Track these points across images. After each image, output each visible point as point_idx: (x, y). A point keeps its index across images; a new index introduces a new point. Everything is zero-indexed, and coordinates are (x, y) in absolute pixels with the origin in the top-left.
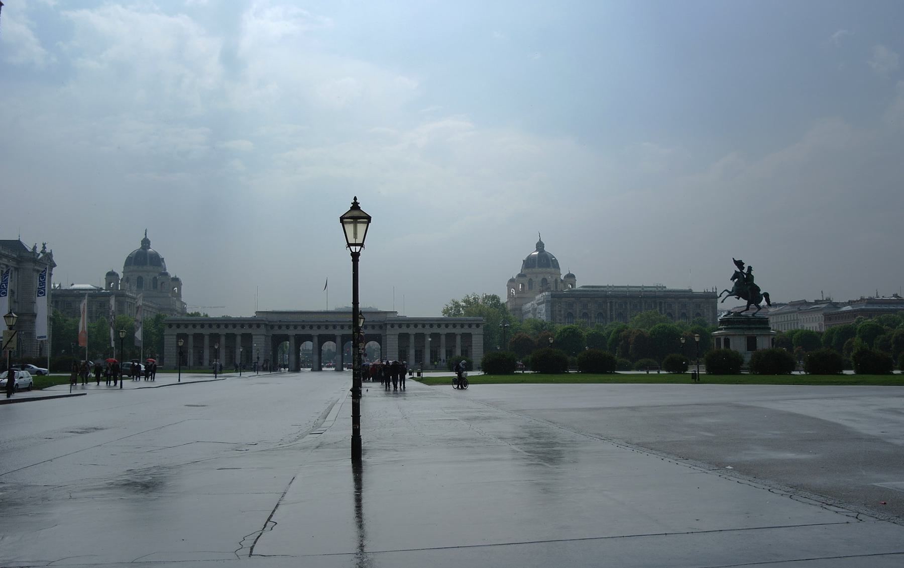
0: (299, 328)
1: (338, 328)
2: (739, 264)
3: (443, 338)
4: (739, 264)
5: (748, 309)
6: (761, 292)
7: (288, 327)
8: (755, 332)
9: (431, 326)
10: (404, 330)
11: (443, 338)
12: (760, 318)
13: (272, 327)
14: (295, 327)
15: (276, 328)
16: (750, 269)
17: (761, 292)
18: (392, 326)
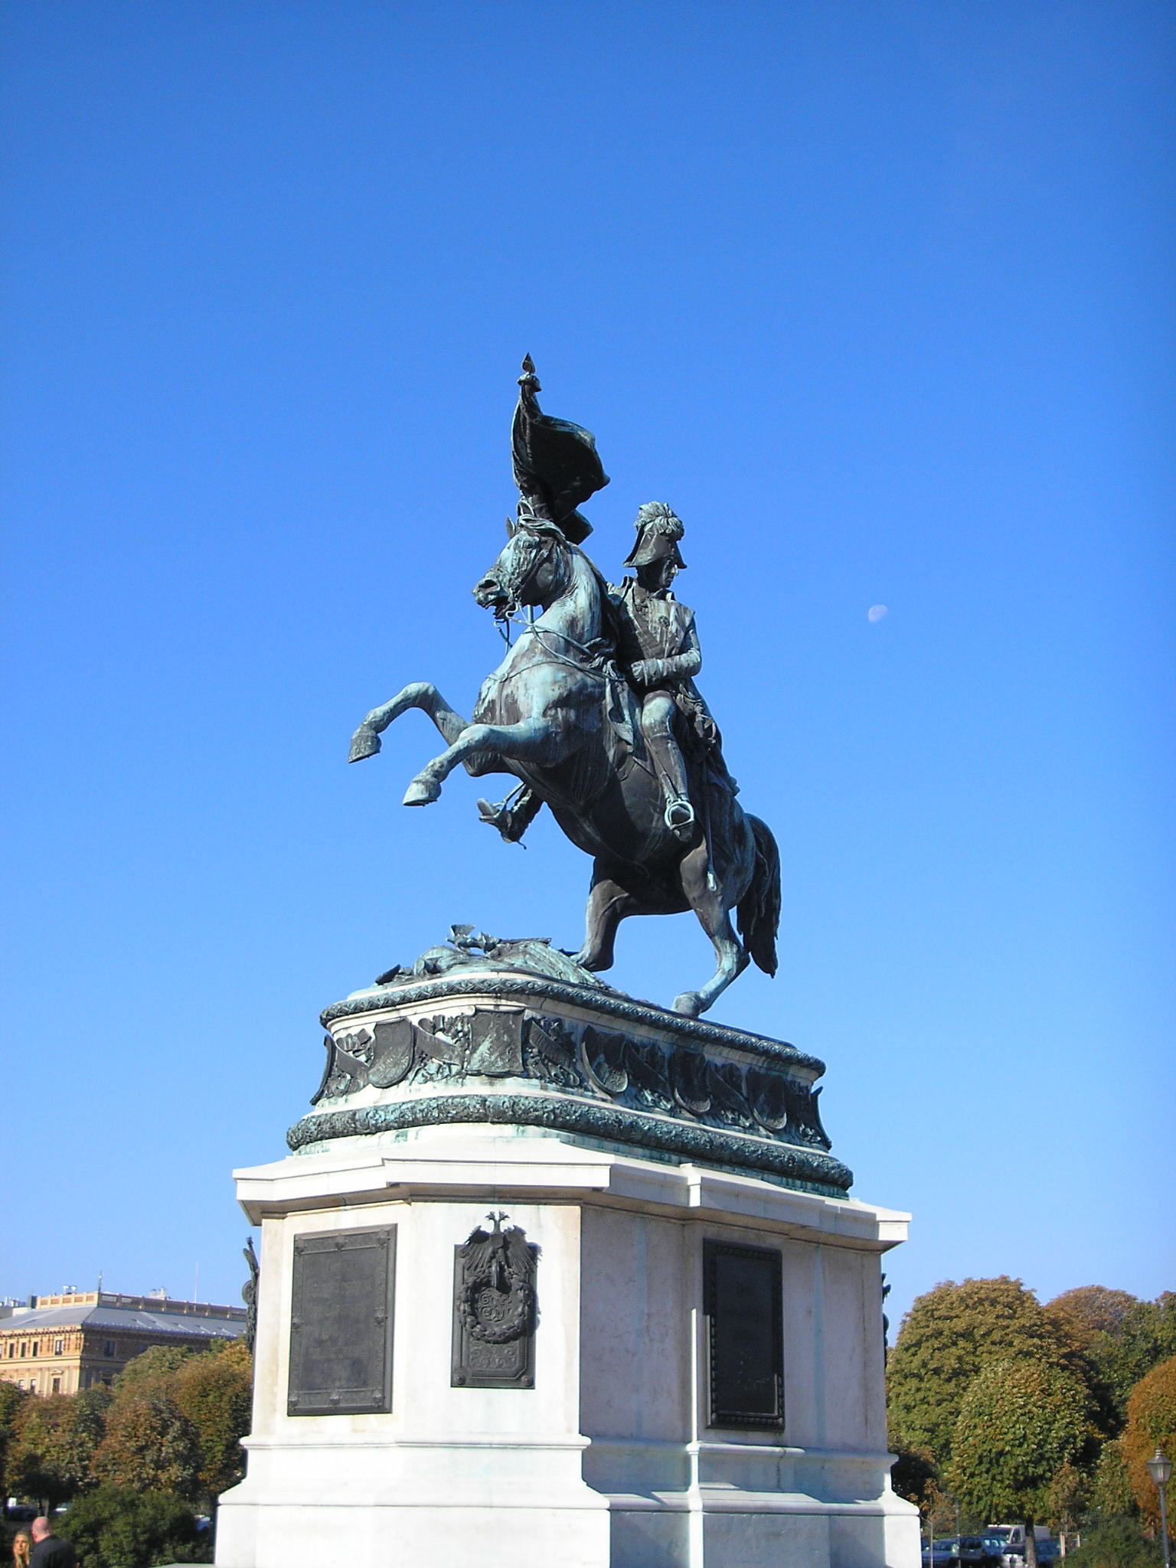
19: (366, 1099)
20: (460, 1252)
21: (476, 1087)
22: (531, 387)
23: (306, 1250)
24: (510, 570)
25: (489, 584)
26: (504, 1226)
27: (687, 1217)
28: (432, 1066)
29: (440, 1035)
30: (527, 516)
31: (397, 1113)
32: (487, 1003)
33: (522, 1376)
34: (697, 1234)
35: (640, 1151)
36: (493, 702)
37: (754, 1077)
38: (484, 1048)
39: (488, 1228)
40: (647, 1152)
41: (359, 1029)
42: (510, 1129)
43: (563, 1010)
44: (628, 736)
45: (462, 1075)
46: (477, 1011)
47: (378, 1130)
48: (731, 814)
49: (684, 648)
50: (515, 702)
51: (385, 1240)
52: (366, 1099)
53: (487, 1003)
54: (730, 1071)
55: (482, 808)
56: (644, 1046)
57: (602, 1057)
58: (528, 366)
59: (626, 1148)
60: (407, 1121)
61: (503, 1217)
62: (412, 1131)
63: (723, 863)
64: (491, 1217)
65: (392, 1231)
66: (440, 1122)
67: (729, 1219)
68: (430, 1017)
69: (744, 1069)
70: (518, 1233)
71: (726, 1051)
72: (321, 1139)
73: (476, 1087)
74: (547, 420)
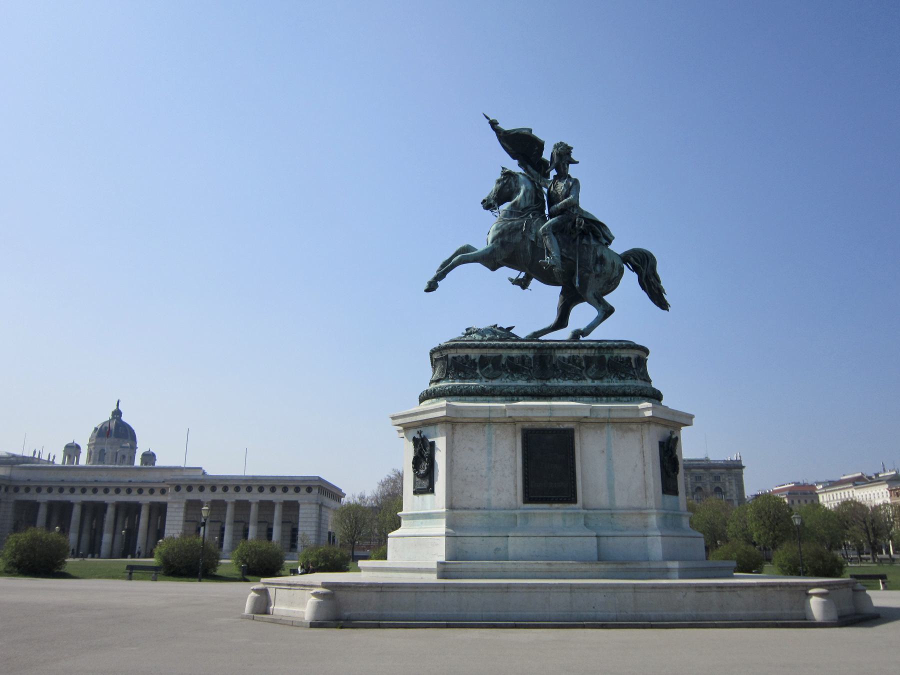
0: (55, 491)
1: (112, 491)
2: (521, 144)
3: (254, 509)
4: (521, 144)
5: (562, 322)
6: (618, 247)
7: (39, 490)
8: (565, 408)
9: (237, 489)
10: (195, 495)
11: (254, 509)
12: (602, 347)
13: (16, 489)
14: (50, 490)
15: (22, 490)
17: (618, 247)
18: (178, 488)
25: (484, 201)
27: (514, 422)
33: (430, 490)
34: (519, 426)
35: (499, 399)
37: (588, 359)
39: (418, 436)
40: (504, 398)
42: (434, 400)
43: (468, 352)
48: (595, 252)
49: (567, 196)
54: (573, 359)
55: (511, 280)
56: (517, 357)
57: (490, 366)
59: (491, 398)
63: (587, 274)
67: (536, 419)
69: (581, 355)
71: (569, 351)
74: (505, 132)
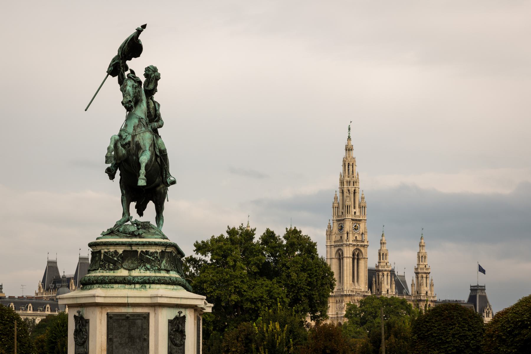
16: (153, 76)
19: (123, 273)
20: (170, 322)
21: (163, 274)
22: (139, 32)
23: (110, 317)
24: (132, 95)
26: (182, 315)
28: (148, 266)
29: (148, 256)
30: (133, 75)
31: (142, 280)
32: (163, 249)
36: (130, 142)
38: (164, 262)
41: (114, 250)
44: (158, 154)
45: (159, 270)
46: (162, 251)
47: (134, 284)
50: (139, 144)
51: (146, 317)
52: (123, 273)
53: (163, 249)
58: (144, 27)
60: (145, 282)
61: (181, 312)
62: (148, 286)
64: (179, 312)
65: (148, 314)
66: (157, 283)
68: (144, 250)
70: (184, 317)
72: (108, 284)
73: (163, 274)
